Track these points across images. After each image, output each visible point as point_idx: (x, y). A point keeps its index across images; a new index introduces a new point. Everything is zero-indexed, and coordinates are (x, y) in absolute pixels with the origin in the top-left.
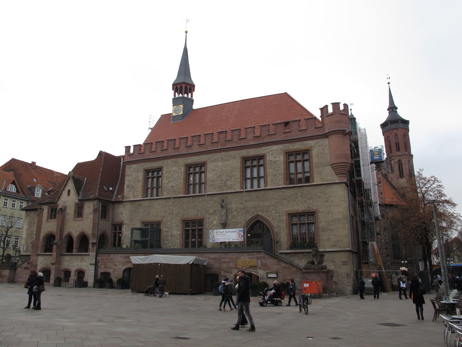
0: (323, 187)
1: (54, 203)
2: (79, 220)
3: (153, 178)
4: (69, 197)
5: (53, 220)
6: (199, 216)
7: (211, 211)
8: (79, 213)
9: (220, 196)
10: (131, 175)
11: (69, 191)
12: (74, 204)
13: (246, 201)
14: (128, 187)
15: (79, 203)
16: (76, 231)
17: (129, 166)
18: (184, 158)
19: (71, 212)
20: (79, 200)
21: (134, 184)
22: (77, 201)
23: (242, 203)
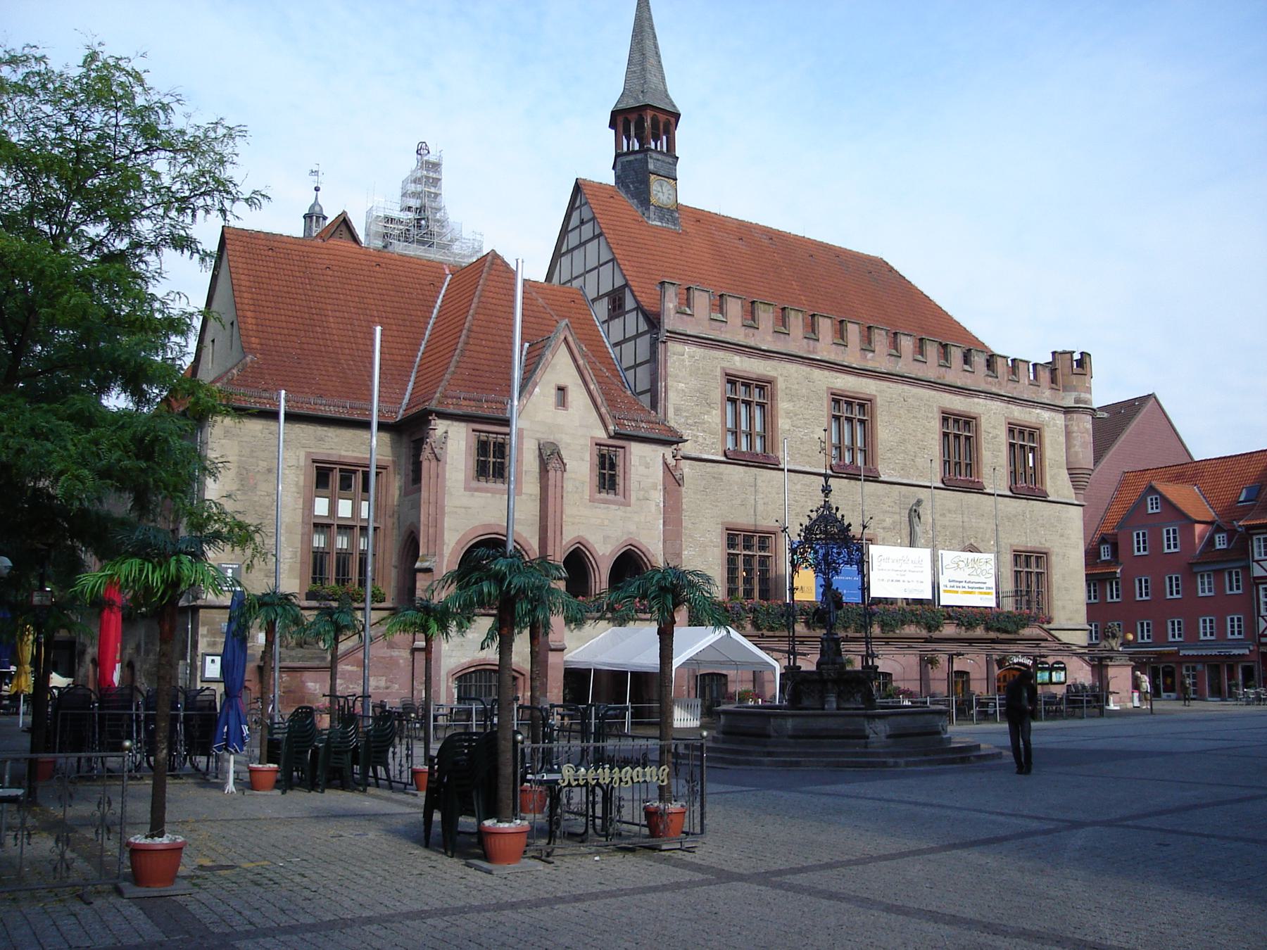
4: (561, 412)
5: (491, 485)
7: (888, 521)
8: (608, 475)
11: (561, 389)
13: (950, 511)
14: (678, 410)
16: (606, 538)
18: (826, 373)
19: (580, 469)
22: (601, 435)
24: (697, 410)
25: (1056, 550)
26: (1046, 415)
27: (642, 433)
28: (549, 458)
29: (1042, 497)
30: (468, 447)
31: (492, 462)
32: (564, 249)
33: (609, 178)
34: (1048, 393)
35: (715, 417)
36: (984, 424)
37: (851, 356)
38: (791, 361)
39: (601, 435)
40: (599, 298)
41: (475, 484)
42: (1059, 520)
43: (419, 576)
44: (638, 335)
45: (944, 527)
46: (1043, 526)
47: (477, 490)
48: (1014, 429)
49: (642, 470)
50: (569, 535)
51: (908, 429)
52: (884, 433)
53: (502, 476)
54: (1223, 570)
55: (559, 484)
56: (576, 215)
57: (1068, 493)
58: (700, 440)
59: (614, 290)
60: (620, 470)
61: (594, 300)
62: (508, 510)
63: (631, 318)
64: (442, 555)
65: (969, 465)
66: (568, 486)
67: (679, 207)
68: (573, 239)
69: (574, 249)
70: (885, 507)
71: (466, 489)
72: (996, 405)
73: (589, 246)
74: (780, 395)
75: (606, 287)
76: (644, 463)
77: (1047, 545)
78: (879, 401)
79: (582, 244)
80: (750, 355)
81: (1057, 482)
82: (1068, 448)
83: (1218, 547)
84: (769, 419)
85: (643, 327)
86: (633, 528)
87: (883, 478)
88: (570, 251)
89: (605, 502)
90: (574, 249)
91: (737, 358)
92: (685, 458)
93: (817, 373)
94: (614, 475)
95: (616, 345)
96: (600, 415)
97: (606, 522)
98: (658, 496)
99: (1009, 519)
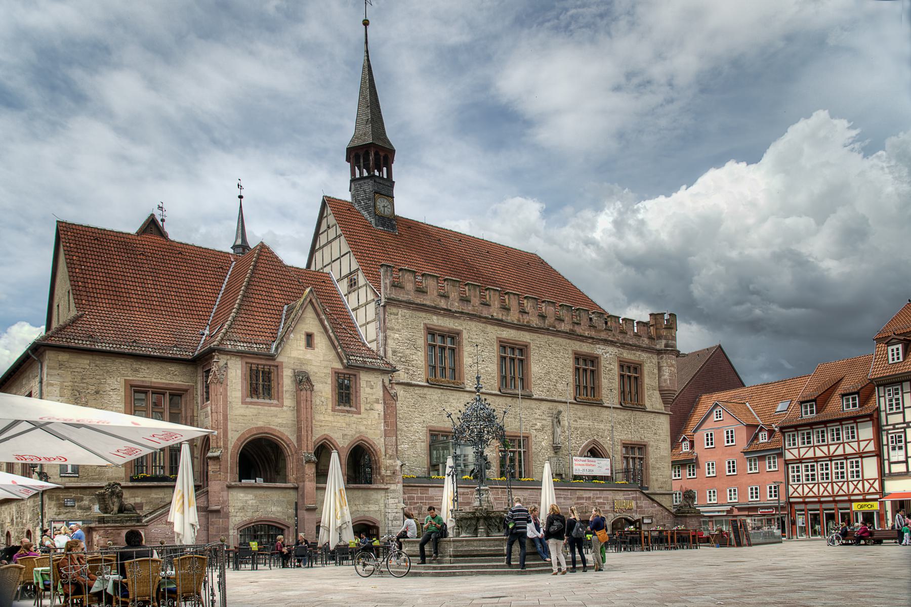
0: (653, 415)
1: (272, 357)
2: (348, 412)
3: (443, 349)
4: (309, 350)
6: (523, 432)
8: (345, 394)
9: (549, 404)
10: (398, 330)
11: (309, 337)
12: (329, 371)
14: (394, 352)
15: (345, 371)
16: (344, 435)
17: (394, 310)
18: (496, 328)
19: (325, 390)
20: (348, 367)
21: (408, 352)
22: (338, 366)
23: (576, 421)
24: (408, 352)
25: (652, 443)
26: (644, 356)
27: (368, 365)
28: (303, 381)
29: (644, 410)
30: (244, 375)
31: (262, 383)
32: (317, 247)
33: (347, 196)
34: (646, 341)
35: (419, 358)
36: (603, 363)
37: (513, 316)
38: (471, 319)
39: (338, 366)
40: (341, 279)
41: (249, 400)
42: (654, 424)
43: (210, 463)
44: (366, 305)
45: (576, 429)
46: (642, 428)
47: (251, 403)
48: (624, 365)
49: (368, 390)
50: (318, 434)
51: (550, 365)
52: (535, 369)
53: (269, 394)
54: (765, 456)
55: (309, 399)
56: (324, 222)
57: (659, 405)
58: (411, 372)
59: (351, 273)
60: (352, 391)
61: (338, 281)
62: (275, 418)
63: (362, 291)
64: (226, 448)
65: (593, 388)
66: (317, 401)
67: (397, 218)
68: (323, 239)
69: (324, 246)
70: (536, 416)
71: (242, 403)
72: (611, 350)
73: (333, 243)
74: (465, 342)
75: (345, 271)
76: (370, 388)
77: (646, 440)
78: (532, 346)
79: (329, 242)
80: (444, 315)
81: (652, 400)
82: (660, 377)
83: (761, 441)
84: (457, 358)
85: (371, 296)
86: (363, 428)
87: (535, 397)
88: (321, 248)
89: (343, 411)
90: (324, 246)
91: (435, 317)
92: (397, 384)
93: (489, 328)
94: (349, 394)
95: (353, 310)
96: (338, 353)
97: (344, 425)
98: (380, 407)
99: (620, 423)
